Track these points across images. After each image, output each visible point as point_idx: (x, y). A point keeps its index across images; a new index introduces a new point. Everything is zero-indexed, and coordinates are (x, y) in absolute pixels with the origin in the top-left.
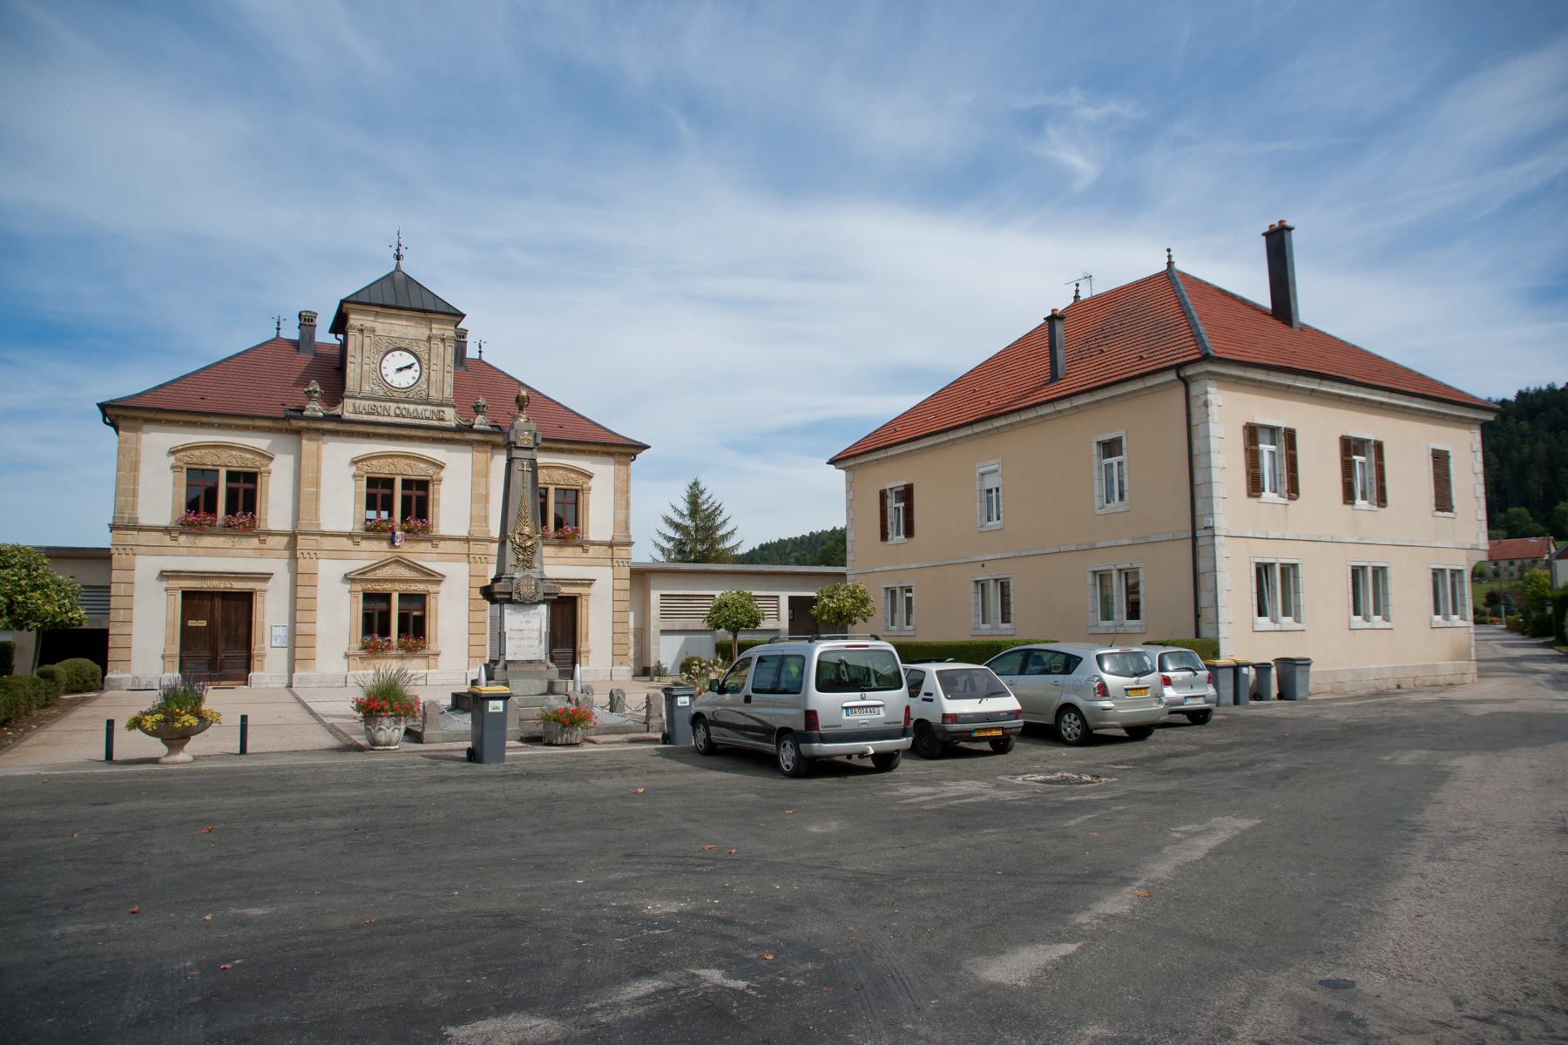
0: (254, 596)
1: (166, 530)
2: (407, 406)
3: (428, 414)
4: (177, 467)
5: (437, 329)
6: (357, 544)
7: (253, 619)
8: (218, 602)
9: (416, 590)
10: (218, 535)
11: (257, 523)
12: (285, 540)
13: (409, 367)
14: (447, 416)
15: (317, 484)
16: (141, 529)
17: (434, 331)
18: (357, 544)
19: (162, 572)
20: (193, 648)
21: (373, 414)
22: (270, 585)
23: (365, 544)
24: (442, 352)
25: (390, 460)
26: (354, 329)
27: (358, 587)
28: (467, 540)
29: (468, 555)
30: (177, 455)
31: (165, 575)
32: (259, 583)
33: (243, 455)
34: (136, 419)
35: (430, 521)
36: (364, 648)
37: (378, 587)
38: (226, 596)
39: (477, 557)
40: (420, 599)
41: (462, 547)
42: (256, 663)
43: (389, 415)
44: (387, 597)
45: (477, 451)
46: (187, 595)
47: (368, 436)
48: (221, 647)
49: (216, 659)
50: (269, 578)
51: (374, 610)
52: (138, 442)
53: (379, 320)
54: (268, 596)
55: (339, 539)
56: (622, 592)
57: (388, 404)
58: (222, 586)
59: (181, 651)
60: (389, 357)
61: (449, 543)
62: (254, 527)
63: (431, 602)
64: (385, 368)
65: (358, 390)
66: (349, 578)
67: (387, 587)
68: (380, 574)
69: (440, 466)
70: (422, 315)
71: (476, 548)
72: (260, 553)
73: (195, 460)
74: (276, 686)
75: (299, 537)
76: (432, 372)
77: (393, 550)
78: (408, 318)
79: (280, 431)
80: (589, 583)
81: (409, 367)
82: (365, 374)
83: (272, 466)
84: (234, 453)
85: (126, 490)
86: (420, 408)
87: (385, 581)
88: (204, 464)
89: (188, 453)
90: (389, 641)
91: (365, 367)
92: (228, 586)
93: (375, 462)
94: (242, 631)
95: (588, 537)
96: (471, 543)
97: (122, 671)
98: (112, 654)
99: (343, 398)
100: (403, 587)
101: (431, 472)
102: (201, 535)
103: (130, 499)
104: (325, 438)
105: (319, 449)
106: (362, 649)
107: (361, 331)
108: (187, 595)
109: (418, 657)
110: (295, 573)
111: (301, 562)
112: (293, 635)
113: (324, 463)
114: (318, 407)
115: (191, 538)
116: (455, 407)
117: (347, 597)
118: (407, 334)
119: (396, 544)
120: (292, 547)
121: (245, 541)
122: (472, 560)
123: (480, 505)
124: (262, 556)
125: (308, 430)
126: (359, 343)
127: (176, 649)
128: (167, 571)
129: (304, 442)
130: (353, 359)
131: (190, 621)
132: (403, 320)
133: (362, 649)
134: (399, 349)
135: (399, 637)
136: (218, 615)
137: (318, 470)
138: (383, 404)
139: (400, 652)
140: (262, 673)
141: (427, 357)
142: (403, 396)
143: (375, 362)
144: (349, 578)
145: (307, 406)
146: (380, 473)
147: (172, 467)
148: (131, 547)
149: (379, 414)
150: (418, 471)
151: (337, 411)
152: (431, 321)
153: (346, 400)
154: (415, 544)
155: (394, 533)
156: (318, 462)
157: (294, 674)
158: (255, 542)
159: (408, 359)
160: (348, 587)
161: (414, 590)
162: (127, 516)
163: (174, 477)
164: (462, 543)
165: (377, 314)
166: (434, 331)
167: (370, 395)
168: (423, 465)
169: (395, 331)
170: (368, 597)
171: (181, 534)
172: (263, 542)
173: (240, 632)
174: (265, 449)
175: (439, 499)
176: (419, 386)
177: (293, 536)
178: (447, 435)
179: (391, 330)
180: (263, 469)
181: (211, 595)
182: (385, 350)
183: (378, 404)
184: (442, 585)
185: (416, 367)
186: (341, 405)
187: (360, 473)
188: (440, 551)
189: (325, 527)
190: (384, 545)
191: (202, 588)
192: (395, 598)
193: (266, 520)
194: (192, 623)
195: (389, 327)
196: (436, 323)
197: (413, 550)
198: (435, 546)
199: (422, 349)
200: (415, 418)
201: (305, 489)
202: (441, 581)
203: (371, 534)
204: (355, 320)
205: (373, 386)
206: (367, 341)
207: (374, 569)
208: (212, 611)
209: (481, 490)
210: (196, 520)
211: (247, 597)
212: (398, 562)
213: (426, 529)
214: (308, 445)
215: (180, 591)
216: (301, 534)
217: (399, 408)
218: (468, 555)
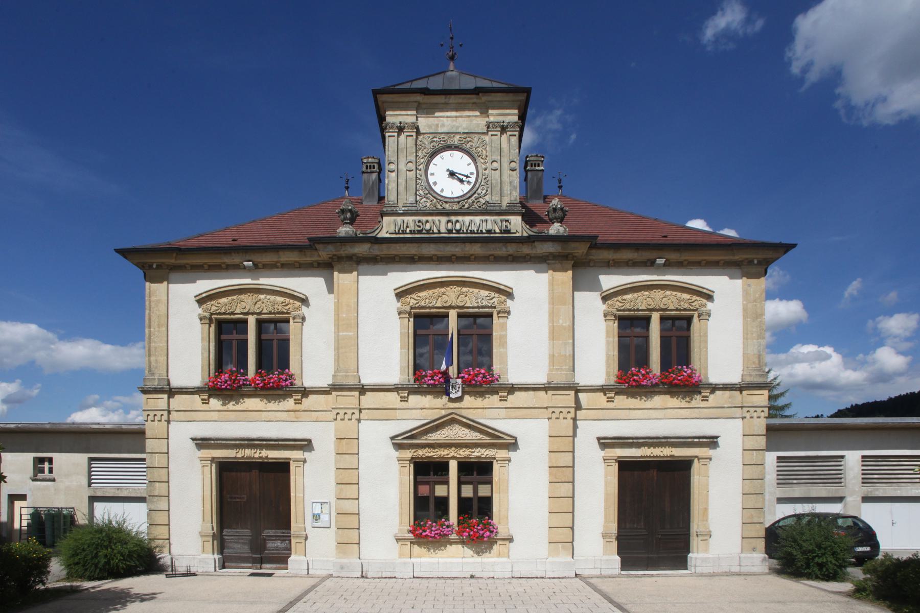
2: (460, 218)
5: (495, 115)
14: (513, 228)
23: (415, 400)
25: (442, 290)
26: (392, 128)
27: (408, 454)
28: (545, 388)
32: (295, 452)
37: (432, 454)
56: (754, 452)
57: (436, 218)
60: (437, 160)
64: (432, 174)
80: (712, 442)
95: (707, 378)
100: (463, 453)
117: (396, 466)
118: (458, 127)
129: (336, 274)
130: (392, 167)
134: (449, 148)
138: (430, 218)
142: (456, 207)
146: (430, 308)
162: (156, 377)
163: (202, 329)
166: (492, 119)
168: (484, 293)
172: (298, 402)
179: (437, 125)
183: (424, 219)
188: (508, 406)
189: (366, 380)
191: (236, 458)
198: (503, 399)
207: (426, 432)
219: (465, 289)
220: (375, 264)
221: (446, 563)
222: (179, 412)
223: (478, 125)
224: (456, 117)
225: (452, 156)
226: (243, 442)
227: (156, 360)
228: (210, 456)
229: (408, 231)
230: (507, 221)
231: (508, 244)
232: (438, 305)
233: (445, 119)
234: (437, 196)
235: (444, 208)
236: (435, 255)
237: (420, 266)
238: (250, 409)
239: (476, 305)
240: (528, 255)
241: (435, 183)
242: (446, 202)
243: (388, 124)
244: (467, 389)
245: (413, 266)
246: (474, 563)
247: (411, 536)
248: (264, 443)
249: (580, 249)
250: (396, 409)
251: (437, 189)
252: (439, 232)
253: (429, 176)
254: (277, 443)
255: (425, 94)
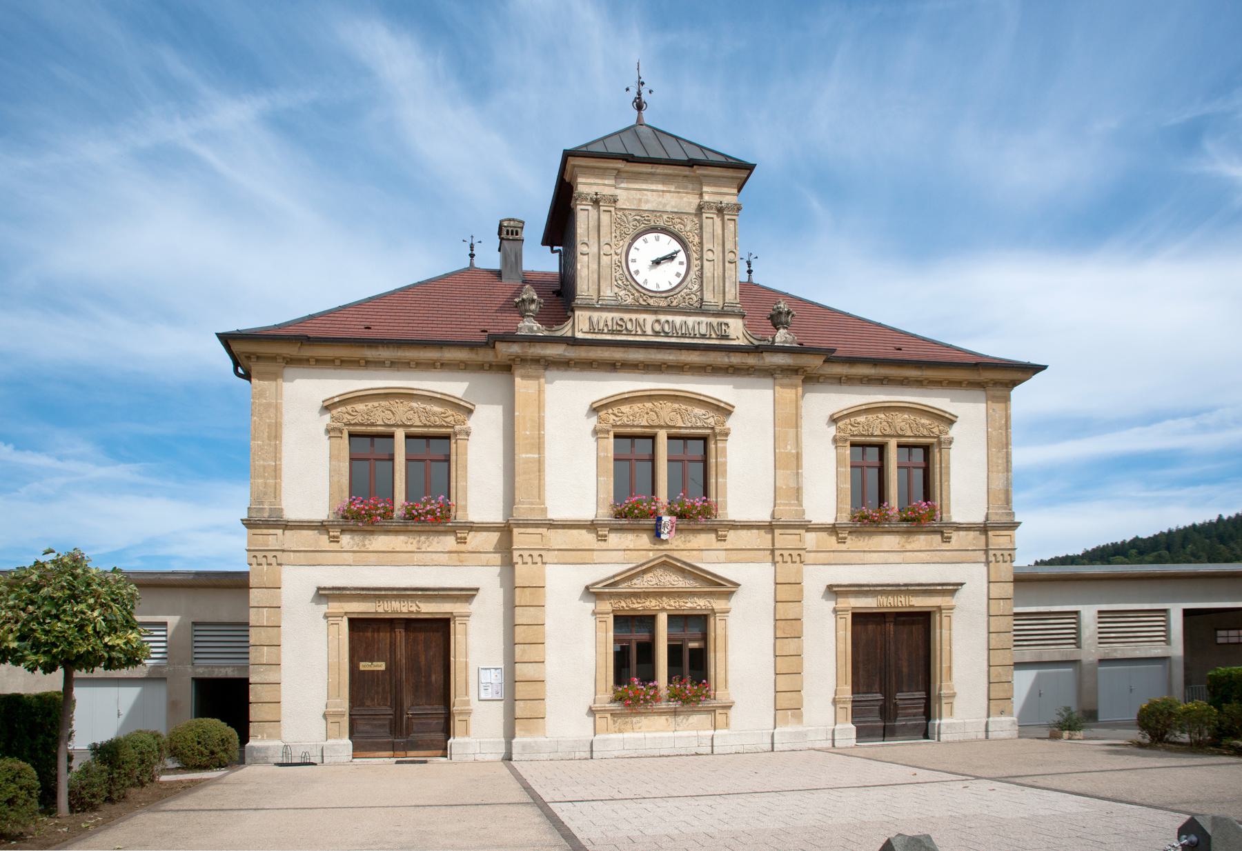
0: (452, 625)
1: (322, 527)
2: (670, 318)
3: (703, 331)
4: (334, 429)
6: (603, 539)
7: (452, 659)
8: (400, 634)
9: (694, 609)
10: (397, 532)
11: (453, 513)
12: (494, 537)
13: (671, 258)
15: (539, 446)
16: (287, 526)
17: (706, 198)
18: (603, 539)
19: (319, 589)
20: (368, 703)
21: (619, 332)
22: (474, 607)
23: (614, 539)
24: (720, 232)
25: (649, 405)
27: (607, 606)
28: (770, 527)
29: (773, 551)
30: (334, 412)
31: (324, 595)
33: (428, 407)
34: (273, 358)
35: (713, 499)
36: (618, 699)
38: (412, 624)
39: (786, 553)
40: (701, 621)
41: (762, 539)
42: (457, 724)
43: (644, 334)
44: (648, 621)
45: (782, 386)
46: (357, 624)
47: (613, 367)
48: (407, 700)
49: (401, 717)
50: (474, 596)
51: (629, 641)
52: (278, 394)
53: (623, 185)
54: (472, 623)
55: (575, 532)
57: (641, 317)
58: (405, 610)
59: (351, 708)
60: (639, 243)
61: (743, 533)
62: (448, 518)
63: (716, 627)
64: (634, 261)
65: (595, 297)
66: (591, 593)
67: (651, 604)
68: (640, 584)
69: (725, 411)
70: (686, 171)
71: (785, 540)
72: (459, 557)
73: (359, 419)
74: (489, 757)
75: (516, 531)
76: (706, 263)
77: (657, 547)
78: (666, 179)
79: (481, 367)
81: (671, 258)
82: (605, 272)
83: (472, 423)
84: (414, 405)
85: (264, 467)
86: (691, 320)
87: (647, 595)
88: (373, 425)
89: (349, 408)
90: (655, 687)
91: (605, 260)
92: (414, 609)
93: (625, 409)
94: (436, 678)
96: (777, 532)
97: (270, 736)
98: (255, 712)
99: (573, 311)
100: (673, 604)
101: (711, 421)
102: (372, 532)
103: (271, 481)
104: (550, 374)
105: (540, 391)
106: (614, 701)
107: (596, 203)
108: (357, 624)
109: (699, 712)
110: (510, 586)
111: (519, 569)
112: (511, 681)
113: (548, 413)
114: (536, 326)
115: (358, 538)
116: (743, 316)
117: (591, 621)
118: (665, 205)
119: (663, 537)
120: (506, 548)
121: (436, 539)
122: (778, 558)
123: (789, 472)
124: (461, 564)
125: (524, 361)
126: (593, 223)
127: (343, 704)
128: (325, 589)
129: (518, 380)
131: (362, 664)
132: (657, 182)
133: (614, 701)
134: (654, 229)
135: (670, 681)
136: (401, 654)
137: (540, 425)
138: (634, 316)
139: (672, 705)
140: (466, 739)
141: (697, 240)
142: (663, 303)
143: (619, 251)
144: (591, 593)
145: (519, 325)
146: (633, 426)
147: (328, 431)
148: (274, 553)
149: (629, 333)
150: (695, 420)
151: (566, 331)
152: (700, 182)
153: (577, 313)
154: (691, 537)
155: (660, 519)
156: (539, 413)
157: (514, 741)
158: (449, 542)
159: (667, 245)
160: (590, 606)
161: (692, 609)
164: (762, 532)
165: (619, 175)
166: (706, 198)
167: (613, 303)
168: (699, 411)
169: (647, 202)
170: (622, 621)
171: (343, 531)
172: (462, 541)
173: (433, 678)
174: (460, 396)
175: (725, 464)
176: (686, 287)
177: (506, 530)
178: (736, 359)
179: (640, 200)
180: (457, 428)
181: (390, 623)
182: (632, 232)
183: (626, 316)
184: (734, 598)
185: (681, 256)
186: (570, 322)
187: (604, 426)
188: (728, 547)
189: (554, 514)
190: (644, 540)
191: (376, 613)
192: (662, 621)
193: (465, 508)
194: (364, 666)
195: (638, 195)
196: (709, 185)
197: (689, 546)
198: (722, 539)
199: (688, 228)
200: (683, 336)
201: (522, 456)
202: (732, 593)
203: (624, 521)
204: (586, 186)
205: (616, 290)
206: (605, 218)
207: (630, 578)
208: (393, 645)
209: (789, 447)
210: (363, 509)
211: (441, 627)
212: (667, 565)
213: (707, 511)
214: (524, 386)
215: (345, 620)
216: (518, 526)
217: (658, 321)
218: (773, 551)
219: (676, 406)
220: (566, 370)
221: (655, 738)
222: (298, 554)
223: (690, 203)
224: (663, 191)
225: (657, 239)
226: (389, 593)
227: (265, 483)
228: (341, 610)
229: (606, 331)
230: (726, 324)
231: (732, 354)
232: (644, 423)
233: (649, 193)
234: (640, 289)
235: (649, 304)
236: (642, 362)
237: (621, 375)
238: (398, 550)
239: (690, 425)
240: (752, 367)
241: (637, 272)
242: (651, 297)
243: (580, 194)
244: (680, 527)
245: (614, 375)
246: (689, 737)
247: (615, 706)
248: (420, 593)
249: (815, 362)
250: (593, 550)
251: (639, 279)
252: (644, 334)
253: (630, 263)
254: (436, 593)
255: (628, 161)
